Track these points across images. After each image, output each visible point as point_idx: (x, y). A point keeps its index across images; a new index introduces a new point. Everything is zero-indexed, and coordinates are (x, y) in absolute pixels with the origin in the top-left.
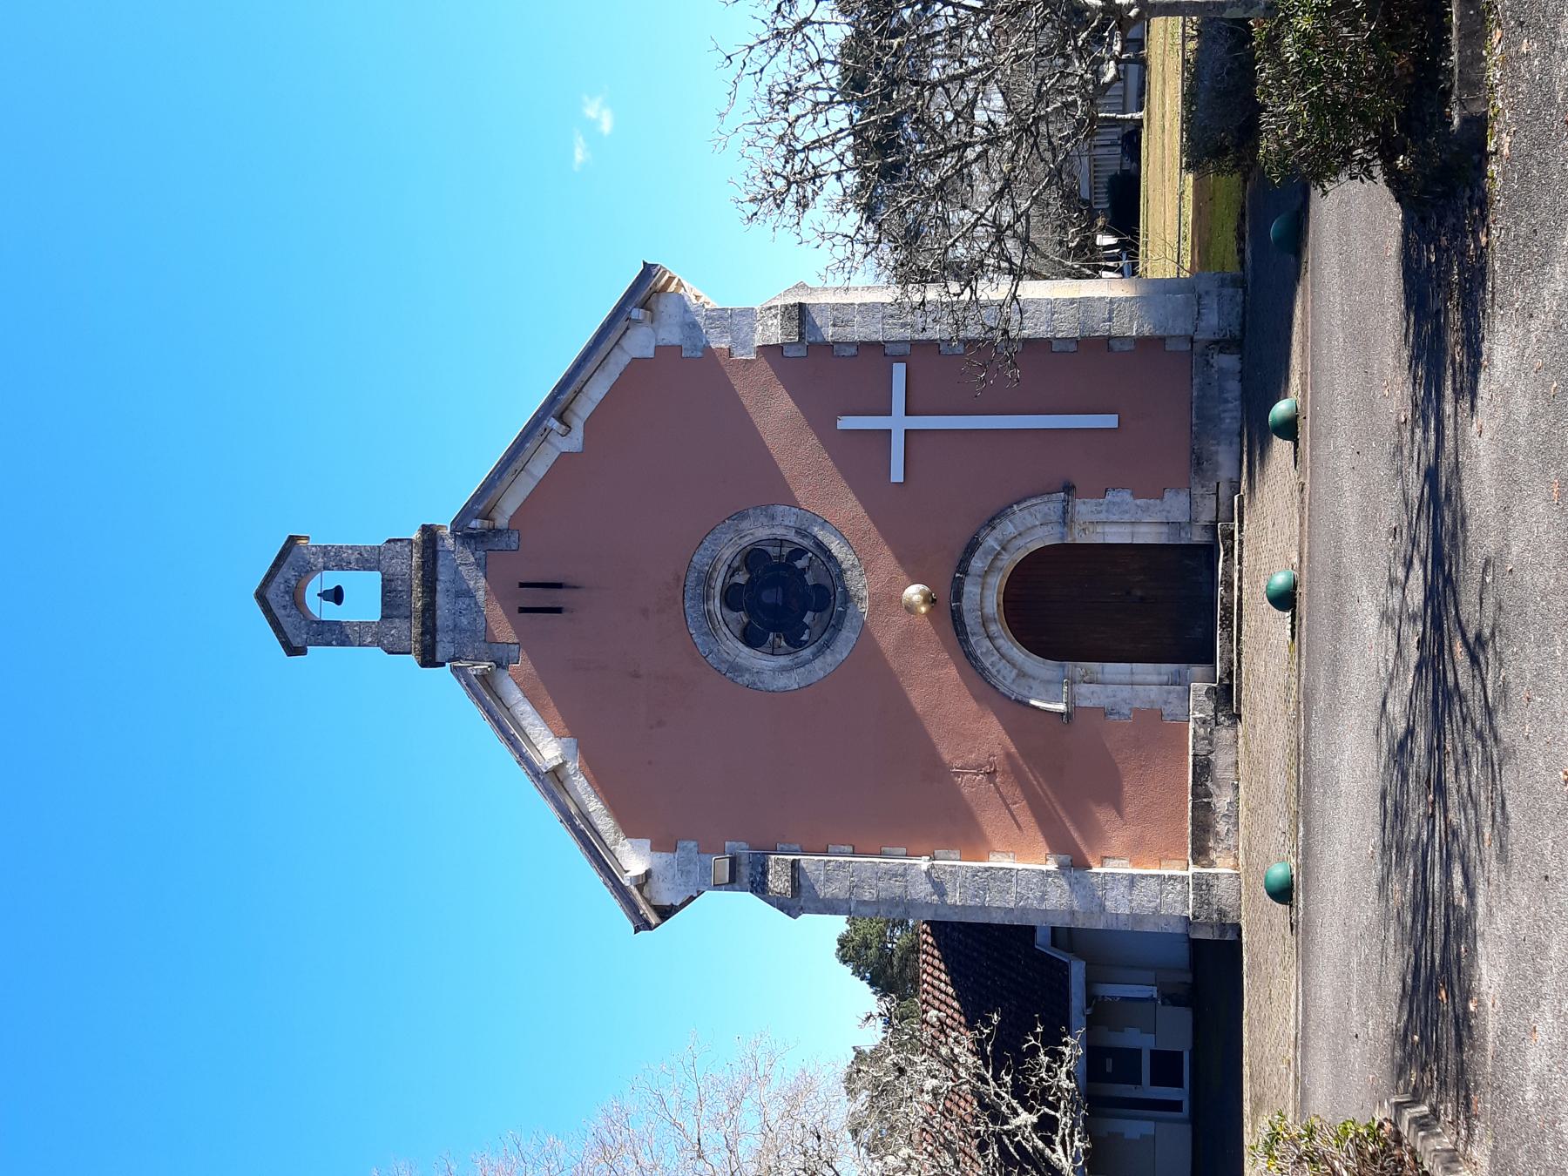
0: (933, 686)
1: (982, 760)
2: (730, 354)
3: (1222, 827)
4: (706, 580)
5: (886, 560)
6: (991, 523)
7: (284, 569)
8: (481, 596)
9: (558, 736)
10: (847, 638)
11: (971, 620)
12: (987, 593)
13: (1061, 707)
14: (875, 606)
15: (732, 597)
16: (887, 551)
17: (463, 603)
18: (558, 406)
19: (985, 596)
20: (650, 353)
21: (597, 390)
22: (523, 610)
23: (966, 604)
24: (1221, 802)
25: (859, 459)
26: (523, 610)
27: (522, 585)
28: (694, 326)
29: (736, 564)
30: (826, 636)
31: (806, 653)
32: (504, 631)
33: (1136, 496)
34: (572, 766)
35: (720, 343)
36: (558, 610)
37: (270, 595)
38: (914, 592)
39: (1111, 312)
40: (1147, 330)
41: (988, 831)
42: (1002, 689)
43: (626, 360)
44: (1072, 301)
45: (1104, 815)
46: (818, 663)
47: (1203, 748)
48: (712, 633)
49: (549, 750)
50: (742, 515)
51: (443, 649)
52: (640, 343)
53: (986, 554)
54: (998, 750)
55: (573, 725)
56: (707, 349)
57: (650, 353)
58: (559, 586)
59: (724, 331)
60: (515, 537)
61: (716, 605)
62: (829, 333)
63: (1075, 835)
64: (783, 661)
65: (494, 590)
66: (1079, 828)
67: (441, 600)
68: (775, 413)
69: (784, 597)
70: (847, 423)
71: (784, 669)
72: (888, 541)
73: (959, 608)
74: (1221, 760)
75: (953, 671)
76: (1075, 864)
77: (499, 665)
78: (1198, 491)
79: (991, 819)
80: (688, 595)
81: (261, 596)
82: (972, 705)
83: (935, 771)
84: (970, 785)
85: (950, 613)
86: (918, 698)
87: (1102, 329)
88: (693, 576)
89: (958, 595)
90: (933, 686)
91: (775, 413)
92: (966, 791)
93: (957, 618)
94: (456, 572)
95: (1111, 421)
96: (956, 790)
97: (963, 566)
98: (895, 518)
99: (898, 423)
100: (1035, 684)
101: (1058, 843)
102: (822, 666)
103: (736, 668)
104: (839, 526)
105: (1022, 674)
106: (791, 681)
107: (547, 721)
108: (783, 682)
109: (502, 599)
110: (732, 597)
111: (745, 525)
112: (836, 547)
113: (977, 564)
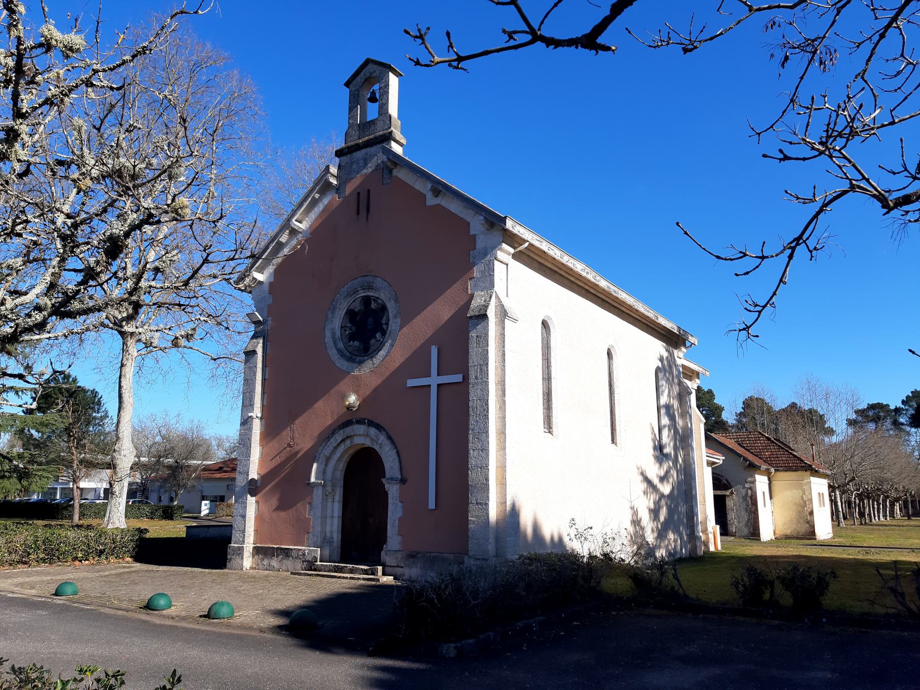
0: (323, 414)
1: (296, 440)
2: (470, 279)
3: (266, 562)
4: (370, 287)
5: (376, 381)
6: (390, 438)
7: (380, 68)
8: (365, 171)
9: (310, 227)
10: (342, 364)
11: (349, 430)
12: (363, 438)
13: (313, 480)
14: (356, 377)
15: (367, 300)
16: (379, 382)
17: (361, 163)
18: (440, 188)
19: (362, 437)
20: (472, 232)
21: (454, 207)
22: (359, 194)
23: (356, 426)
24: (275, 563)
25: (417, 363)
26: (359, 194)
27: (369, 191)
28: (485, 255)
29: (379, 301)
30: (348, 354)
31: (341, 345)
32: (350, 188)
33: (400, 519)
34: (300, 237)
35: (476, 272)
36: (358, 213)
37: (370, 67)
38: (352, 399)
39: (481, 504)
40: (471, 526)
41: (270, 445)
42: (320, 449)
43: (469, 219)
44: (487, 480)
45: (274, 502)
46: (335, 351)
47: (294, 554)
48: (349, 295)
49: (303, 225)
50: (396, 301)
51: (345, 159)
52: (477, 225)
53: (376, 436)
54: (298, 448)
55: (316, 233)
56: (474, 264)
57: (472, 232)
58: (368, 210)
59: (483, 272)
60: (389, 181)
61: (362, 294)
62: (473, 334)
63: (269, 487)
64: (338, 333)
65: (368, 177)
66: (270, 490)
67: (363, 151)
68: (441, 311)
69: (366, 328)
70: (434, 350)
71: (333, 334)
72: (384, 381)
73: (364, 423)
74: (289, 563)
75: (329, 422)
76: (253, 488)
77: (337, 189)
78: (399, 556)
79: (275, 445)
80: (364, 278)
81: (368, 62)
82: (316, 434)
83: (292, 417)
84: (286, 433)
85: (349, 419)
86: (320, 404)
87: (472, 499)
88: (370, 279)
89: (360, 422)
90: (323, 414)
91: (441, 311)
92: (285, 433)
93: (348, 423)
94: (374, 156)
95: (432, 505)
96: (284, 428)
97: (371, 424)
98: (392, 384)
99: (434, 380)
100: (323, 466)
101: (266, 478)
102: (333, 353)
103: (333, 311)
104: (390, 355)
105: (328, 459)
106: (328, 340)
107: (316, 219)
108: (328, 334)
109: (362, 183)
110: (367, 300)
111: (392, 302)
112: (382, 353)
113: (373, 431)
